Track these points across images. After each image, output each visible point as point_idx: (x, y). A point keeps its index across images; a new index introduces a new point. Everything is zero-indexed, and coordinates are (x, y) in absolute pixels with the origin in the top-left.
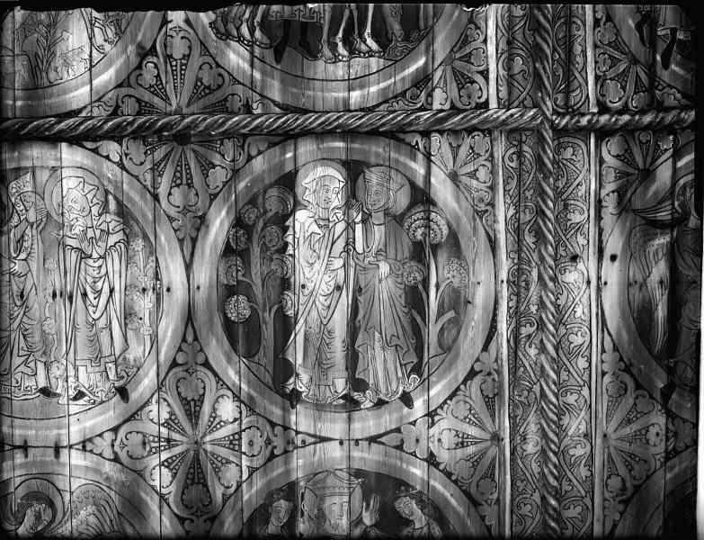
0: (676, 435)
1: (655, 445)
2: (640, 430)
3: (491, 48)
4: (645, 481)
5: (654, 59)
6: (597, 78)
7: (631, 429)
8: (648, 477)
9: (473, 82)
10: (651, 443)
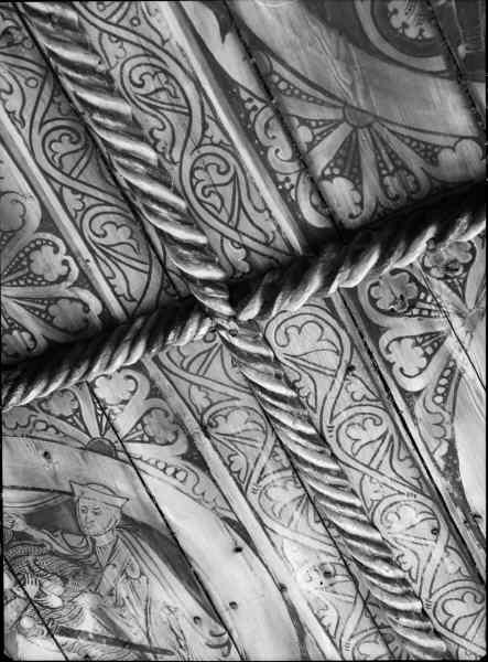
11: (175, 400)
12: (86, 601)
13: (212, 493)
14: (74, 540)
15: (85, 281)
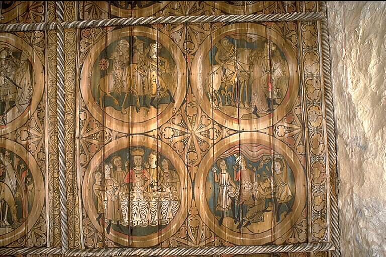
3: (48, 225)
5: (104, 230)
6: (84, 237)
9: (42, 237)
11: (46, 40)
12: (13, 73)
13: (43, 60)
14: (18, 60)
15: (44, 15)
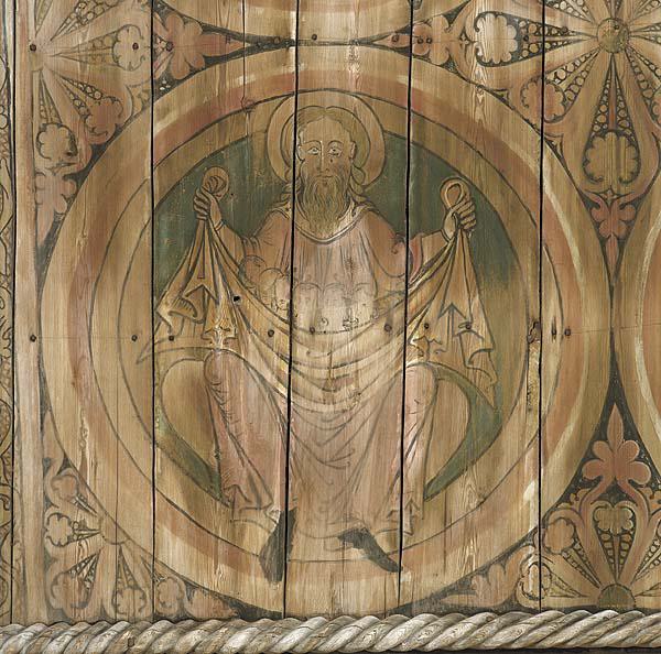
0: (170, 46)
1: (130, 68)
2: (101, 39)
4: (115, 135)
7: (84, 36)
8: (118, 130)
10: (124, 62)
